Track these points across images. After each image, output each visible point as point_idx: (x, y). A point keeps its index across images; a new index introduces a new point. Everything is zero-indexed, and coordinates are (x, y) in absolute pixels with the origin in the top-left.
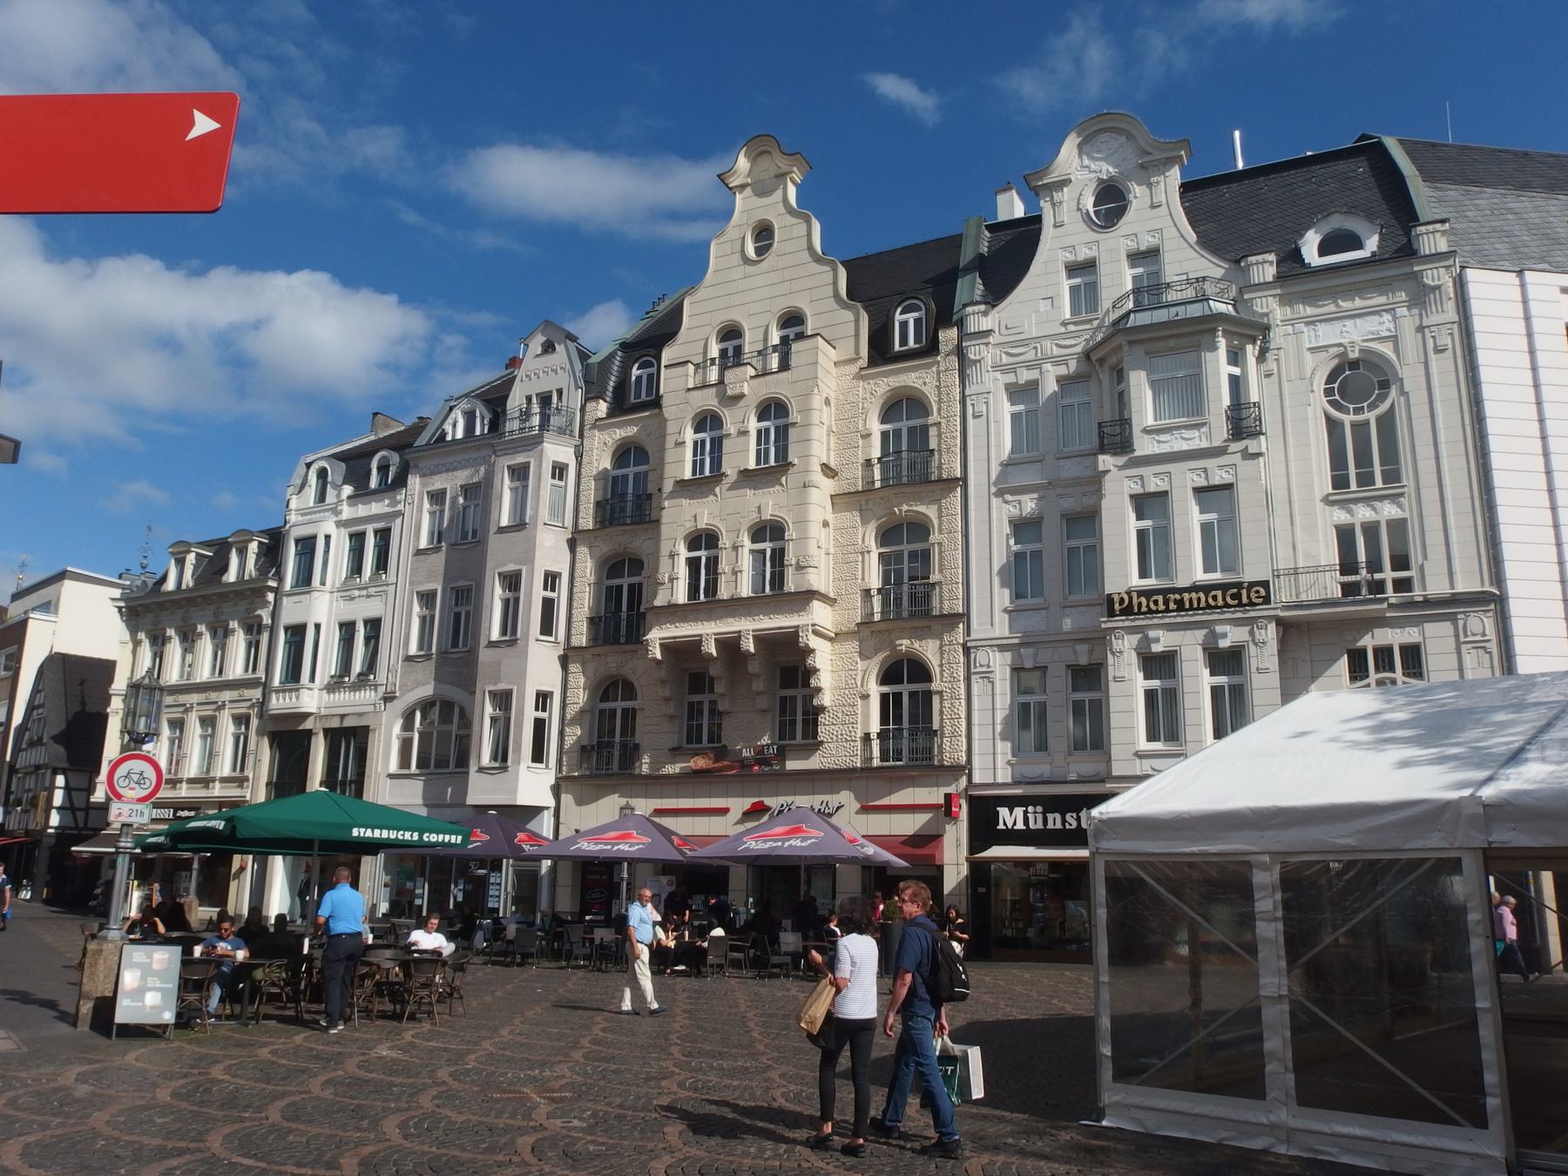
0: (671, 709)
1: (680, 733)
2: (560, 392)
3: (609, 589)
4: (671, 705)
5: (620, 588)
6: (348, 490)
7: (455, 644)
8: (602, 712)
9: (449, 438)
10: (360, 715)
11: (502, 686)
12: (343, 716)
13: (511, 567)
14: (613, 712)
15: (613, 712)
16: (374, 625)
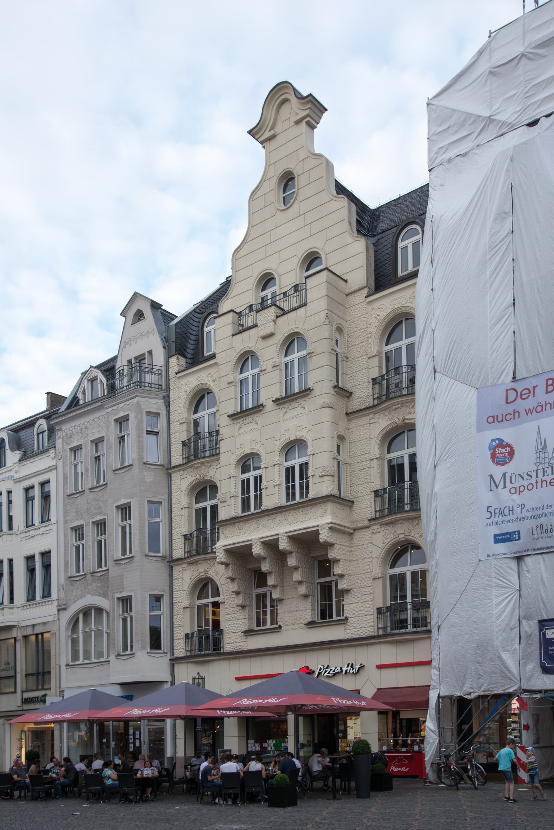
0: (239, 600)
1: (250, 618)
2: (150, 352)
3: (197, 511)
4: (240, 597)
5: (205, 509)
6: (18, 454)
7: (100, 566)
8: (392, 577)
9: (81, 402)
10: (44, 624)
11: (124, 594)
12: (34, 626)
13: (123, 501)
14: (402, 577)
15: (402, 577)
16: (46, 555)
